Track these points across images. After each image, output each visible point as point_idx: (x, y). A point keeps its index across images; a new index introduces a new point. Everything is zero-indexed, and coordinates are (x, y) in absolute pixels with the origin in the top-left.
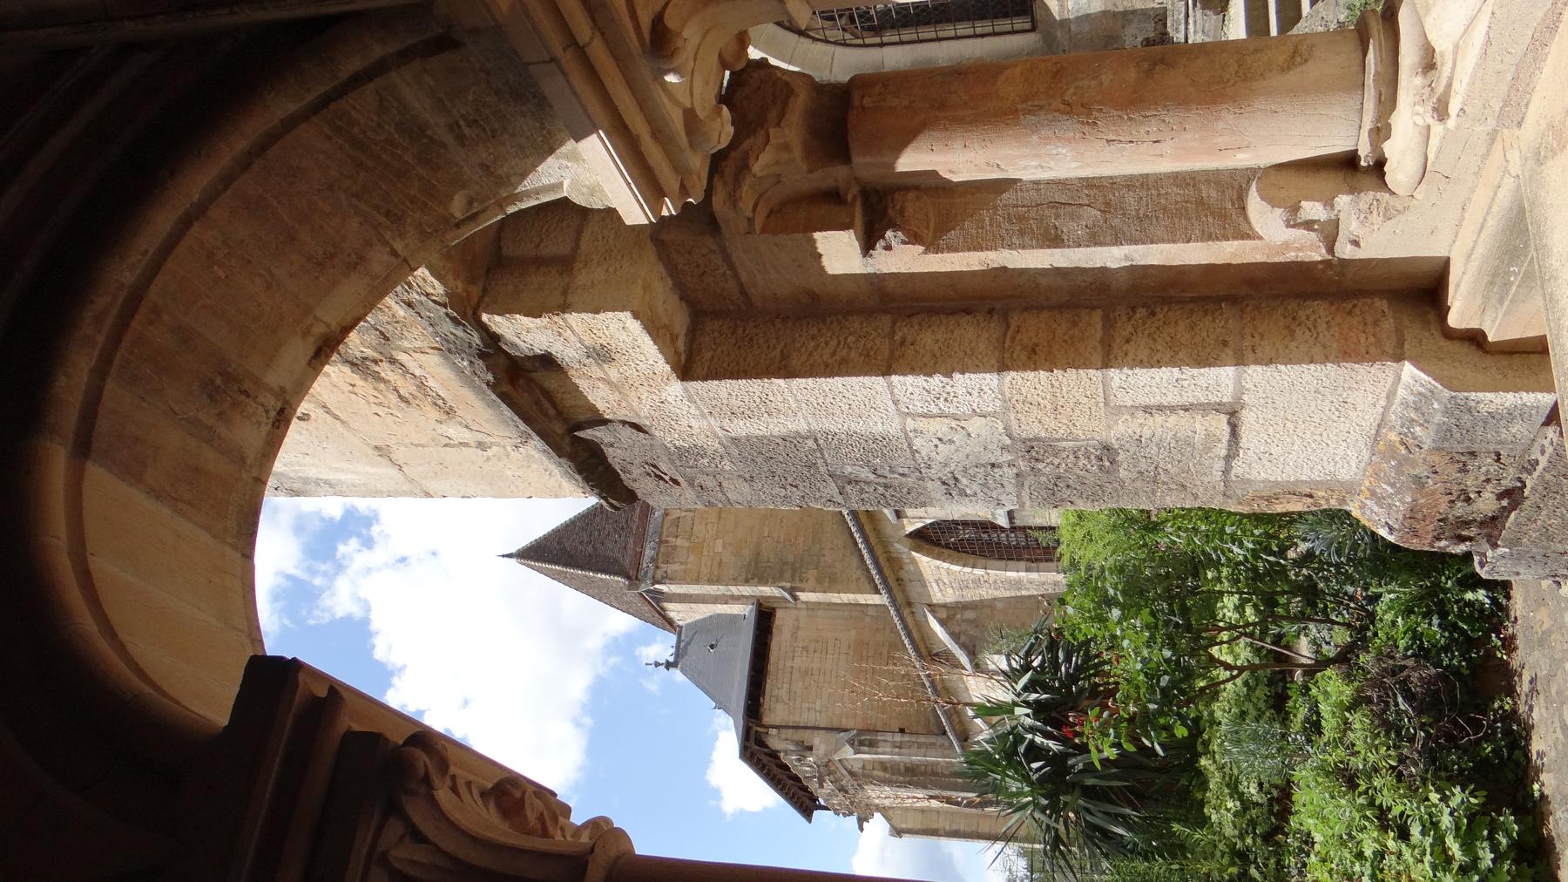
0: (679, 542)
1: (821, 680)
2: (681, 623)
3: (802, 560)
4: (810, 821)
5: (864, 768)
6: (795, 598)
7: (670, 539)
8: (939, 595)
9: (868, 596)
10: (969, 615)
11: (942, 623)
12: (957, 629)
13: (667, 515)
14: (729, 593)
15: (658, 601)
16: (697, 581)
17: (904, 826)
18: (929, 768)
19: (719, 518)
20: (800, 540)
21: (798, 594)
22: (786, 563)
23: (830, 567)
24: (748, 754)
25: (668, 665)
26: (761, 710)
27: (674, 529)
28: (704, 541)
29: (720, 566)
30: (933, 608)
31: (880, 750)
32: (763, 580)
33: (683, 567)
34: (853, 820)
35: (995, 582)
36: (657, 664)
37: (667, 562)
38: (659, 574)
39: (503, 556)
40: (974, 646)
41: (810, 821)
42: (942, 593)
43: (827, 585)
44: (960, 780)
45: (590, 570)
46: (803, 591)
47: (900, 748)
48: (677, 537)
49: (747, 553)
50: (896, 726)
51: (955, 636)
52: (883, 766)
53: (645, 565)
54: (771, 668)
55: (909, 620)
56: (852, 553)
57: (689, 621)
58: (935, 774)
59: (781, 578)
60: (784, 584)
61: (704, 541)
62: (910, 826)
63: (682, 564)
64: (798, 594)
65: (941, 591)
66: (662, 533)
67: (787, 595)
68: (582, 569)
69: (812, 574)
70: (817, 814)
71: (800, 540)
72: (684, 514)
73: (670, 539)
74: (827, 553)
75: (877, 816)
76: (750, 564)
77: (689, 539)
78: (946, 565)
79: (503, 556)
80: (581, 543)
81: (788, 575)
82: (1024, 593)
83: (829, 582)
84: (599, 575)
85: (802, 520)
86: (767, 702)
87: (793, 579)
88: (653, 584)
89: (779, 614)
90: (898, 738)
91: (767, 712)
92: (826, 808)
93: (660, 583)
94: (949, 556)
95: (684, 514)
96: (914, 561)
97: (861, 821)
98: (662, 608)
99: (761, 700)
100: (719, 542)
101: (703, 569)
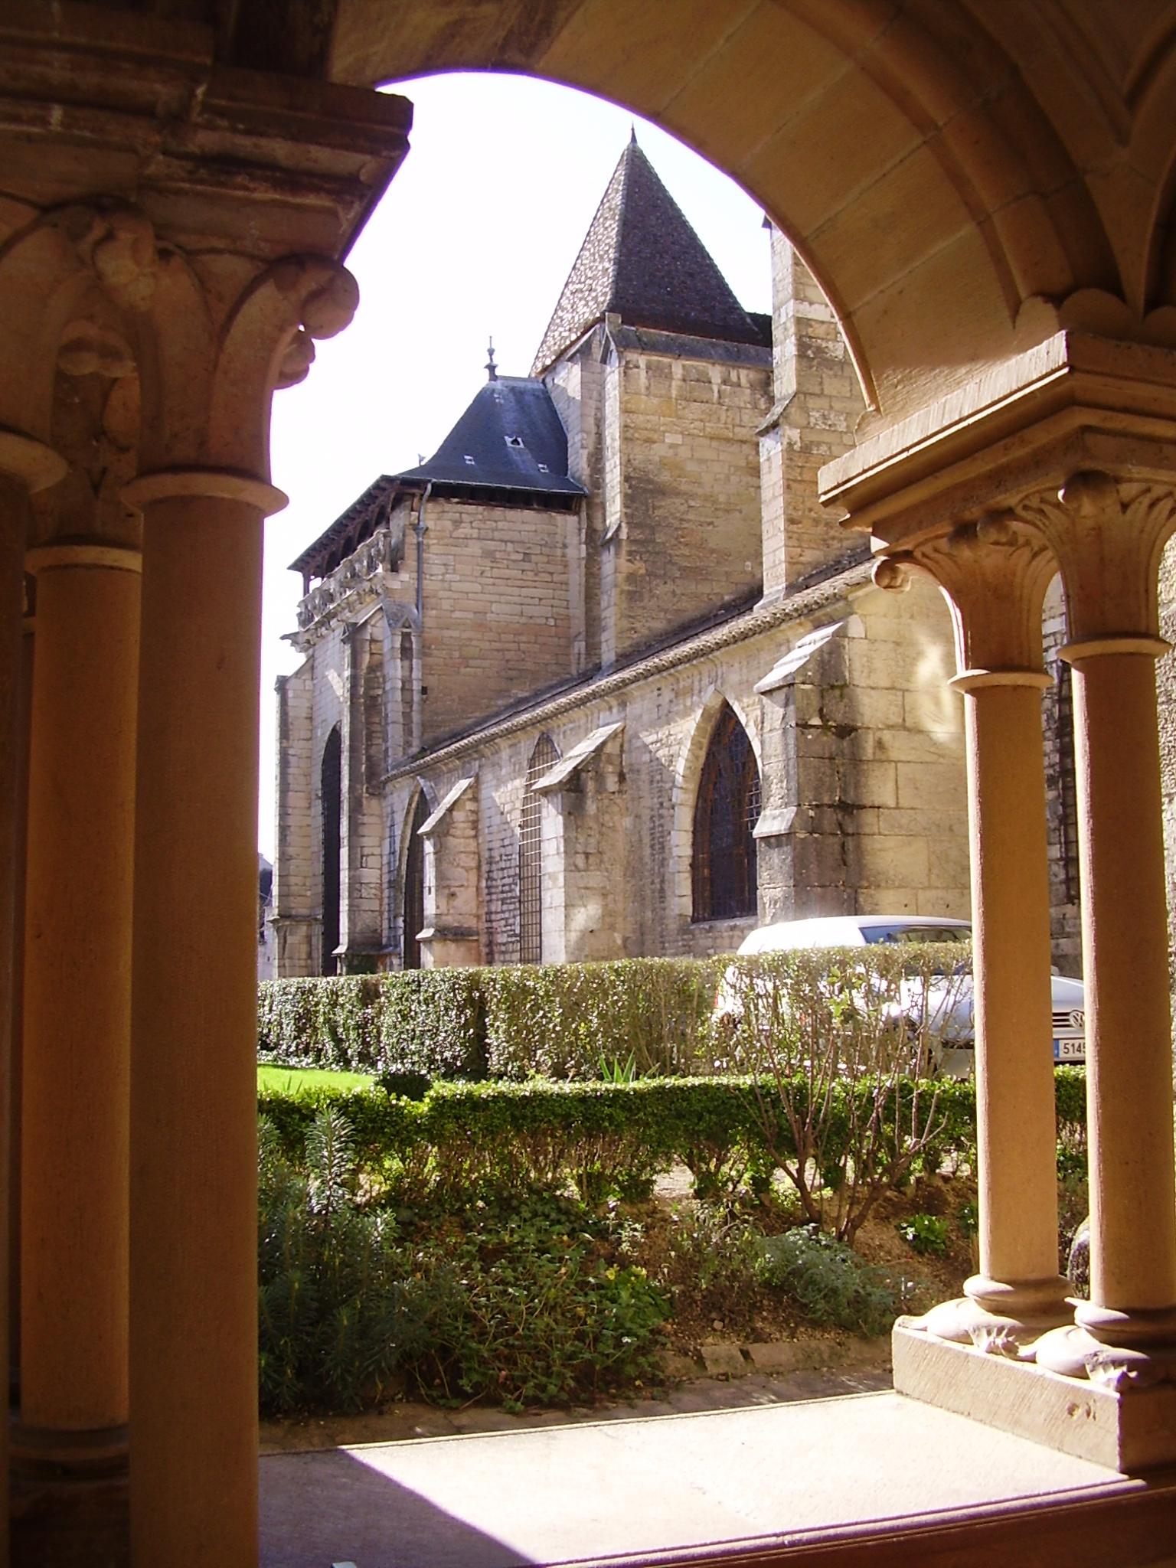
1: (484, 580)
3: (658, 553)
4: (289, 568)
5: (373, 641)
9: (612, 643)
16: (625, 411)
17: (290, 694)
18: (377, 728)
19: (712, 438)
20: (686, 552)
23: (651, 591)
24: (383, 484)
25: (491, 368)
26: (441, 500)
27: (694, 375)
28: (679, 418)
32: (629, 500)
33: (643, 390)
34: (294, 627)
35: (661, 817)
36: (491, 352)
37: (648, 368)
39: (633, 130)
41: (289, 568)
43: (626, 588)
47: (403, 689)
48: (684, 380)
49: (665, 477)
50: (432, 681)
52: (376, 668)
54: (498, 512)
56: (669, 621)
58: (369, 737)
61: (679, 418)
62: (291, 702)
63: (648, 388)
69: (640, 567)
70: (298, 576)
71: (686, 552)
72: (715, 388)
74: (670, 586)
75: (300, 659)
76: (650, 482)
78: (685, 752)
79: (633, 130)
81: (638, 535)
85: (713, 551)
86: (454, 509)
87: (635, 542)
90: (416, 686)
91: (439, 509)
92: (306, 590)
94: (697, 758)
95: (715, 388)
96: (687, 712)
97: (293, 638)
99: (456, 500)
101: (641, 418)
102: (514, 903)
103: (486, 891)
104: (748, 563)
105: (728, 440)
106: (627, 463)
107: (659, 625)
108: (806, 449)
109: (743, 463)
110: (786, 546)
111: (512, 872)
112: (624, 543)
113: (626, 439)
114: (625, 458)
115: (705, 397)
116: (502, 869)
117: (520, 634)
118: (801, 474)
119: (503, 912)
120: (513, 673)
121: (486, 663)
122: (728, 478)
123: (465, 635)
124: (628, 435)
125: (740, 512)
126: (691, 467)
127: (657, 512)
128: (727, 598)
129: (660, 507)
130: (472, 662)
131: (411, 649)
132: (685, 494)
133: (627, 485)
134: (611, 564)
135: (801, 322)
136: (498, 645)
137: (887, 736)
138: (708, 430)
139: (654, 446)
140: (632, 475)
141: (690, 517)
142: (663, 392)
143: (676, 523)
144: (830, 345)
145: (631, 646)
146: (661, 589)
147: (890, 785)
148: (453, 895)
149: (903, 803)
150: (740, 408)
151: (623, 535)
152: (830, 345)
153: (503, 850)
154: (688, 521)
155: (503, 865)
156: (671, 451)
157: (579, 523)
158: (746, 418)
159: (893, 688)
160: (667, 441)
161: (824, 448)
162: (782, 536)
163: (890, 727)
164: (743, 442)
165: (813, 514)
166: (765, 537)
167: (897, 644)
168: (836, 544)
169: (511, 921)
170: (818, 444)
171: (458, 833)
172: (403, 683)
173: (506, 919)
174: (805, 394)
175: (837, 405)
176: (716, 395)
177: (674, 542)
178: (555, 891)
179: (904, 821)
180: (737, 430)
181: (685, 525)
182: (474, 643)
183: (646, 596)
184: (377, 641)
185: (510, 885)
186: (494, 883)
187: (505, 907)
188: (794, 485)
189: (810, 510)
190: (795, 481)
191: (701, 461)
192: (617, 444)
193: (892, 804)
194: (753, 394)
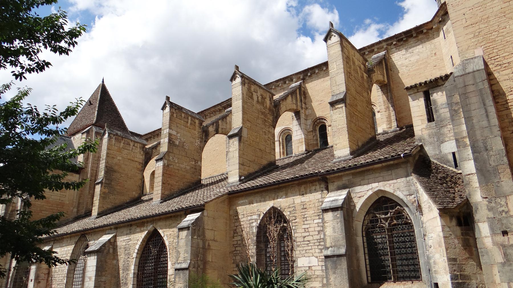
0: (122, 144)
2: (72, 138)
3: (112, 187)
5: (14, 203)
6: (98, 184)
7: (123, 141)
8: (122, 239)
10: (111, 251)
11: (109, 240)
12: (106, 246)
13: (131, 141)
14: (101, 159)
15: (88, 132)
19: (129, 159)
20: (119, 187)
21: (100, 185)
22: (111, 181)
27: (126, 143)
29: (112, 158)
30: (115, 237)
32: (106, 172)
37: (115, 139)
38: (112, 136)
39: (103, 79)
40: (100, 252)
42: (122, 241)
43: (102, 196)
45: (98, 109)
46: (101, 187)
48: (124, 144)
49: (116, 168)
51: (104, 245)
53: (115, 131)
55: (109, 227)
57: (73, 142)
59: (106, 179)
60: (104, 180)
63: (115, 144)
64: (100, 185)
66: (125, 138)
67: (100, 181)
68: (99, 106)
69: (107, 190)
71: (119, 187)
72: (131, 147)
73: (123, 141)
74: (114, 197)
76: (112, 168)
77: (123, 148)
78: (139, 243)
79: (103, 79)
80: (107, 107)
81: (107, 182)
82: (121, 272)
83: (103, 197)
84: (96, 112)
85: (125, 188)
88: (108, 133)
93: (109, 135)
94: (143, 245)
95: (131, 147)
96: (142, 231)
98: (83, 133)
100: (121, 158)
101: (112, 151)
102: (63, 285)
104: (134, 192)
105: (133, 160)
106: (107, 162)
107: (109, 206)
108: (168, 166)
110: (162, 190)
111: (63, 275)
112: (103, 184)
114: (106, 162)
115: (128, 149)
117: (58, 205)
118: (166, 172)
121: (47, 213)
122: (131, 170)
124: (108, 155)
125: (134, 179)
126: (123, 166)
127: (114, 176)
128: (128, 201)
129: (114, 175)
130: (43, 212)
132: (121, 172)
133: (106, 168)
134: (98, 188)
135: (170, 135)
136: (51, 208)
137: (210, 242)
138: (128, 157)
139: (115, 159)
140: (108, 166)
142: (118, 146)
143: (117, 180)
145: (101, 211)
147: (211, 256)
148: (39, 282)
149: (213, 261)
150: (136, 153)
151: (104, 182)
155: (60, 273)
156: (118, 161)
157: (79, 177)
159: (212, 230)
161: (172, 166)
162: (161, 187)
163: (211, 240)
164: (136, 161)
165: (168, 182)
166: (155, 186)
167: (214, 218)
168: (173, 190)
170: (171, 165)
174: (169, 152)
175: (176, 156)
178: (90, 282)
179: (213, 265)
180: (135, 158)
181: (120, 181)
182: (44, 206)
183: (107, 198)
184: (15, 203)
185: (62, 280)
186: (55, 279)
188: (165, 175)
189: (168, 181)
190: (165, 173)
191: (126, 165)
192: (105, 157)
193: (211, 261)
194: (140, 150)
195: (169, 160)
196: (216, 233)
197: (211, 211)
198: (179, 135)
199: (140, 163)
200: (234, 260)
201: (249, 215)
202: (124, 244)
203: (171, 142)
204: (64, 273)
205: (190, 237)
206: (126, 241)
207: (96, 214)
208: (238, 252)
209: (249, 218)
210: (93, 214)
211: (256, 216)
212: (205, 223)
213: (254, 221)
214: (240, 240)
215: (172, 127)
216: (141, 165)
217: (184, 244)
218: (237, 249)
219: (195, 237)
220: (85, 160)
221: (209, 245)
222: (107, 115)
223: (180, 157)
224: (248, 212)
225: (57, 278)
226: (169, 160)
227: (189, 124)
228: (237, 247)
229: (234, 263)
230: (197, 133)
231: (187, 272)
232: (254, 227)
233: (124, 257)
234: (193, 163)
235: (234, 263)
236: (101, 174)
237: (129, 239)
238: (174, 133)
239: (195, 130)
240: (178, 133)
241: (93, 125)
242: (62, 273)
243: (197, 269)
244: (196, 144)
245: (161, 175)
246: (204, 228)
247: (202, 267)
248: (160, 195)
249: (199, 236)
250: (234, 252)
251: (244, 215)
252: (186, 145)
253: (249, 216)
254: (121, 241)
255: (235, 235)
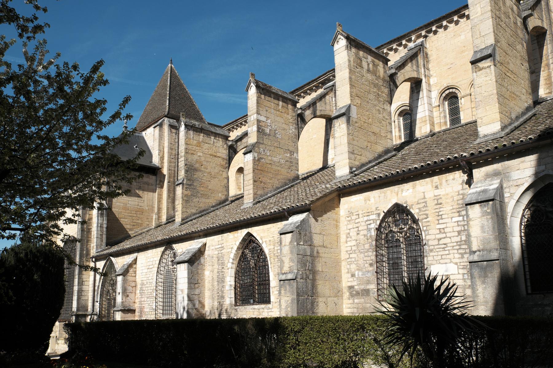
3: (194, 189)
20: (202, 189)
21: (181, 186)
31: (99, 218)
32: (186, 171)
35: (222, 272)
44: (85, 252)
46: (183, 189)
47: (101, 227)
49: (197, 165)
60: (185, 181)
63: (193, 138)
65: (216, 249)
67: (180, 182)
69: (189, 192)
71: (202, 189)
72: (212, 140)
74: (197, 199)
76: (193, 166)
77: (202, 141)
83: (186, 200)
85: (210, 190)
87: (188, 185)
89: (154, 177)
94: (238, 253)
95: (212, 140)
100: (201, 154)
101: (191, 146)
103: (140, 294)
104: (220, 194)
105: (215, 156)
106: (186, 160)
108: (259, 160)
109: (219, 164)
110: (253, 189)
111: (152, 288)
113: (186, 153)
115: (210, 142)
116: (147, 287)
119: (147, 301)
120: (135, 224)
121: (126, 220)
123: (120, 211)
124: (187, 151)
126: (204, 163)
127: (195, 176)
128: (214, 204)
129: (195, 175)
131: (103, 214)
135: (258, 121)
137: (319, 248)
141: (204, 178)
142: (198, 139)
143: (200, 180)
144: (266, 129)
146: (196, 200)
149: (323, 270)
152: (266, 129)
153: (148, 281)
154: (203, 180)
155: (148, 285)
158: (220, 150)
160: (198, 154)
161: (263, 160)
162: (252, 186)
163: (320, 246)
164: (219, 157)
169: (151, 304)
170: (262, 158)
171: (130, 275)
172: (101, 225)
173: (149, 304)
175: (268, 147)
176: (212, 142)
177: (199, 186)
180: (218, 153)
185: (151, 292)
187: (148, 300)
188: (256, 170)
190: (256, 169)
191: (207, 162)
195: (259, 153)
196: (325, 237)
197: (318, 211)
198: (269, 121)
199: (223, 159)
200: (348, 269)
201: (364, 215)
202: (217, 252)
203: (260, 130)
204: (153, 285)
205: (295, 243)
206: (218, 249)
207: (180, 220)
208: (353, 260)
209: (366, 218)
210: (177, 220)
211: (375, 215)
212: (312, 227)
213: (372, 222)
214: (354, 246)
215: (261, 112)
216: (225, 161)
217: (289, 252)
218: (351, 256)
219: (302, 243)
220: (160, 159)
221: (318, 252)
222: (180, 104)
223: (273, 148)
224: (364, 212)
225: (146, 291)
226: (259, 153)
227: (280, 107)
228: (351, 253)
229: (348, 272)
230: (290, 118)
231: (294, 284)
232: (373, 229)
233: (217, 267)
234: (288, 155)
235: (348, 272)
236: (182, 174)
237: (221, 248)
238: (262, 118)
239: (288, 114)
240: (267, 118)
241: (166, 116)
242: (150, 285)
243: (306, 280)
244: (291, 132)
245: (251, 170)
246: (310, 232)
247: (311, 277)
248: (252, 195)
249: (305, 242)
250: (349, 260)
251: (358, 215)
252: (279, 133)
253: (365, 216)
254: (213, 249)
255: (349, 239)
